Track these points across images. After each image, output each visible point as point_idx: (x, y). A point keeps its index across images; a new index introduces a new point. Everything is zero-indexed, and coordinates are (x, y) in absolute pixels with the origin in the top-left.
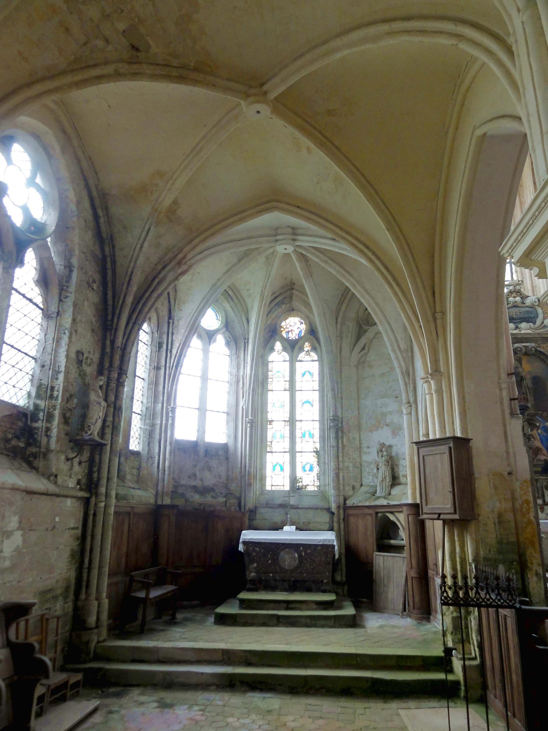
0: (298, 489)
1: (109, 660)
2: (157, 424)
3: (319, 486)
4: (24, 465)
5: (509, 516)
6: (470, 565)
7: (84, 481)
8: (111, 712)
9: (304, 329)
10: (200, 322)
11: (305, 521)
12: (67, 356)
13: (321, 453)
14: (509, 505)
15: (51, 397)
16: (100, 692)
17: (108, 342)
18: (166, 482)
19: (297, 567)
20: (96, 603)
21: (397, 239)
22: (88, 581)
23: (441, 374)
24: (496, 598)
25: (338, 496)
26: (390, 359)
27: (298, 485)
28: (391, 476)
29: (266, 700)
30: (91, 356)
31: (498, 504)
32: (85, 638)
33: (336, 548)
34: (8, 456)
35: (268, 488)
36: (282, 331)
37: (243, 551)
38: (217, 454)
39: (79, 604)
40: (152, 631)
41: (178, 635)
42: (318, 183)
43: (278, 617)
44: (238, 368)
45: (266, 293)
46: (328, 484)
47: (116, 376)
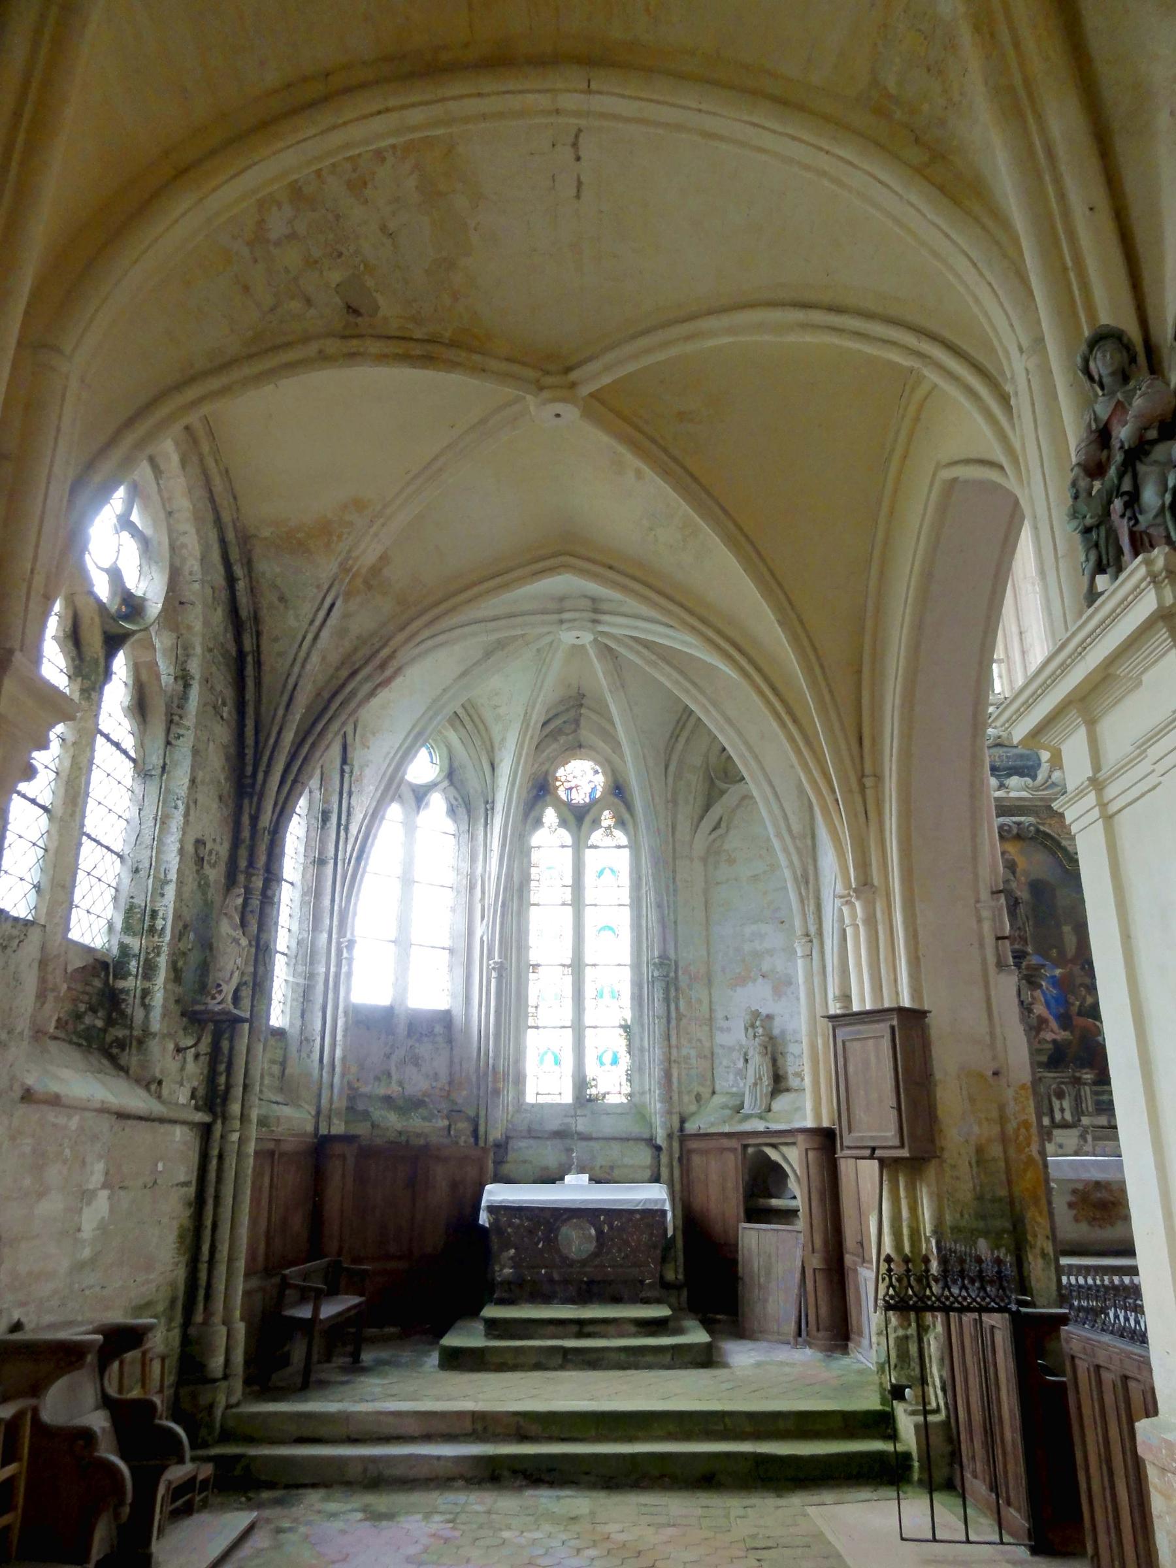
0: (590, 1100)
1: (251, 1440)
2: (318, 974)
3: (630, 1095)
4: (105, 1062)
5: (996, 1151)
6: (928, 1241)
7: (201, 1092)
8: (279, 1531)
9: (602, 784)
10: (405, 773)
11: (604, 1163)
12: (181, 851)
13: (636, 1029)
14: (996, 1130)
15: (152, 930)
16: (243, 1499)
17: (246, 820)
18: (336, 1091)
19: (596, 1254)
20: (223, 1330)
21: (795, 639)
22: (209, 1285)
23: (873, 889)
24: (978, 1296)
25: (670, 1113)
26: (770, 849)
27: (588, 1092)
28: (771, 1074)
29: (562, 1501)
30: (217, 847)
31: (976, 1129)
32: (204, 1400)
33: (669, 1215)
34: (80, 1045)
35: (530, 1098)
36: (558, 787)
37: (487, 1225)
38: (431, 1033)
39: (192, 1331)
40: (323, 1384)
41: (378, 1390)
42: (651, 529)
43: (565, 1351)
44: (473, 860)
45: (534, 717)
46: (650, 1090)
47: (261, 886)
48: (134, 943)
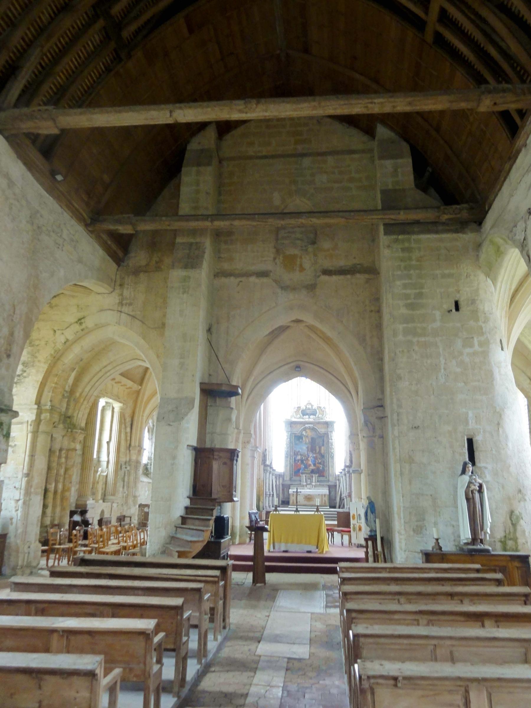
48: (149, 462)
